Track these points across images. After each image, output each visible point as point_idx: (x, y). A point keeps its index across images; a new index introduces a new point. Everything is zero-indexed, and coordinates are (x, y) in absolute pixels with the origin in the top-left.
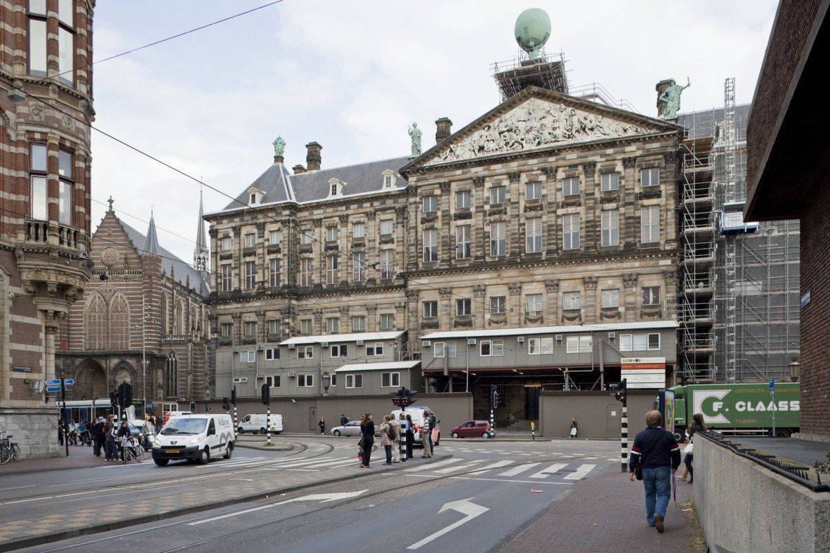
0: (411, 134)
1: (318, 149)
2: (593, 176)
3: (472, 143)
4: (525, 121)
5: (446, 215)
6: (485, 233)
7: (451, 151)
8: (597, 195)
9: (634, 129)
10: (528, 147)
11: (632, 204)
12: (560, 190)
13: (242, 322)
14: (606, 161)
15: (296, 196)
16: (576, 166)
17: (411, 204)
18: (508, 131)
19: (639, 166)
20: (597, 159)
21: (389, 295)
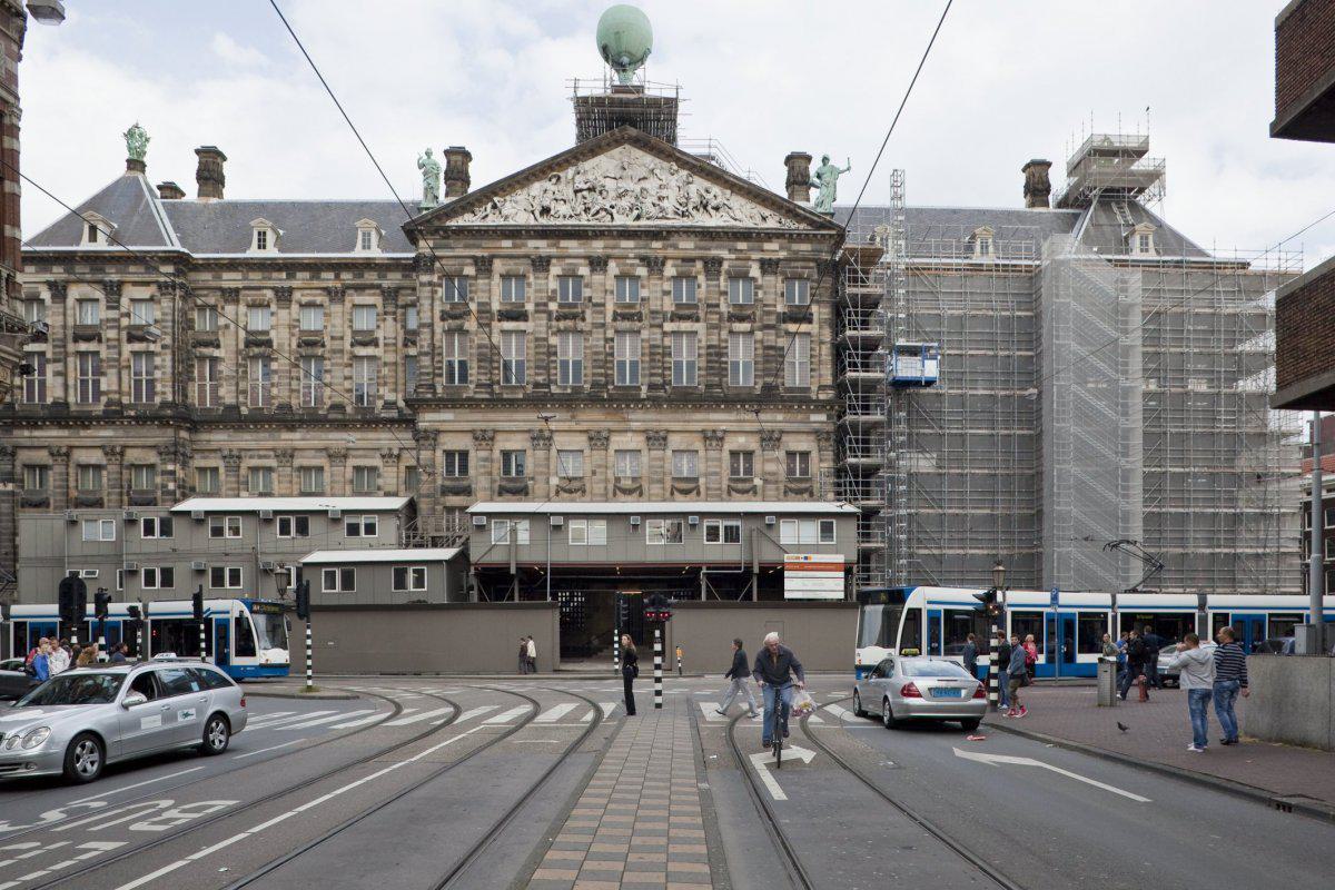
0: (421, 166)
1: (219, 160)
2: (718, 279)
3: (531, 199)
5: (484, 309)
6: (549, 346)
7: (495, 207)
8: (723, 308)
10: (621, 220)
12: (667, 293)
13: (71, 465)
14: (737, 259)
15: (180, 239)
16: (692, 260)
17: (422, 284)
18: (589, 189)
19: (783, 273)
20: (724, 254)
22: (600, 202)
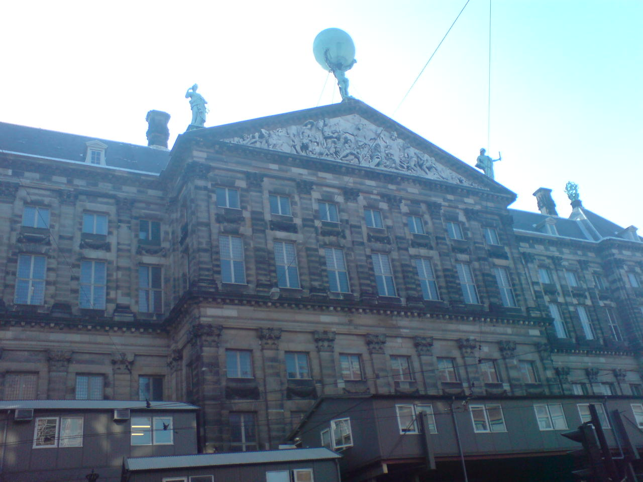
5: (257, 218)
6: (320, 257)
11: (484, 259)
20: (439, 201)
21: (101, 339)
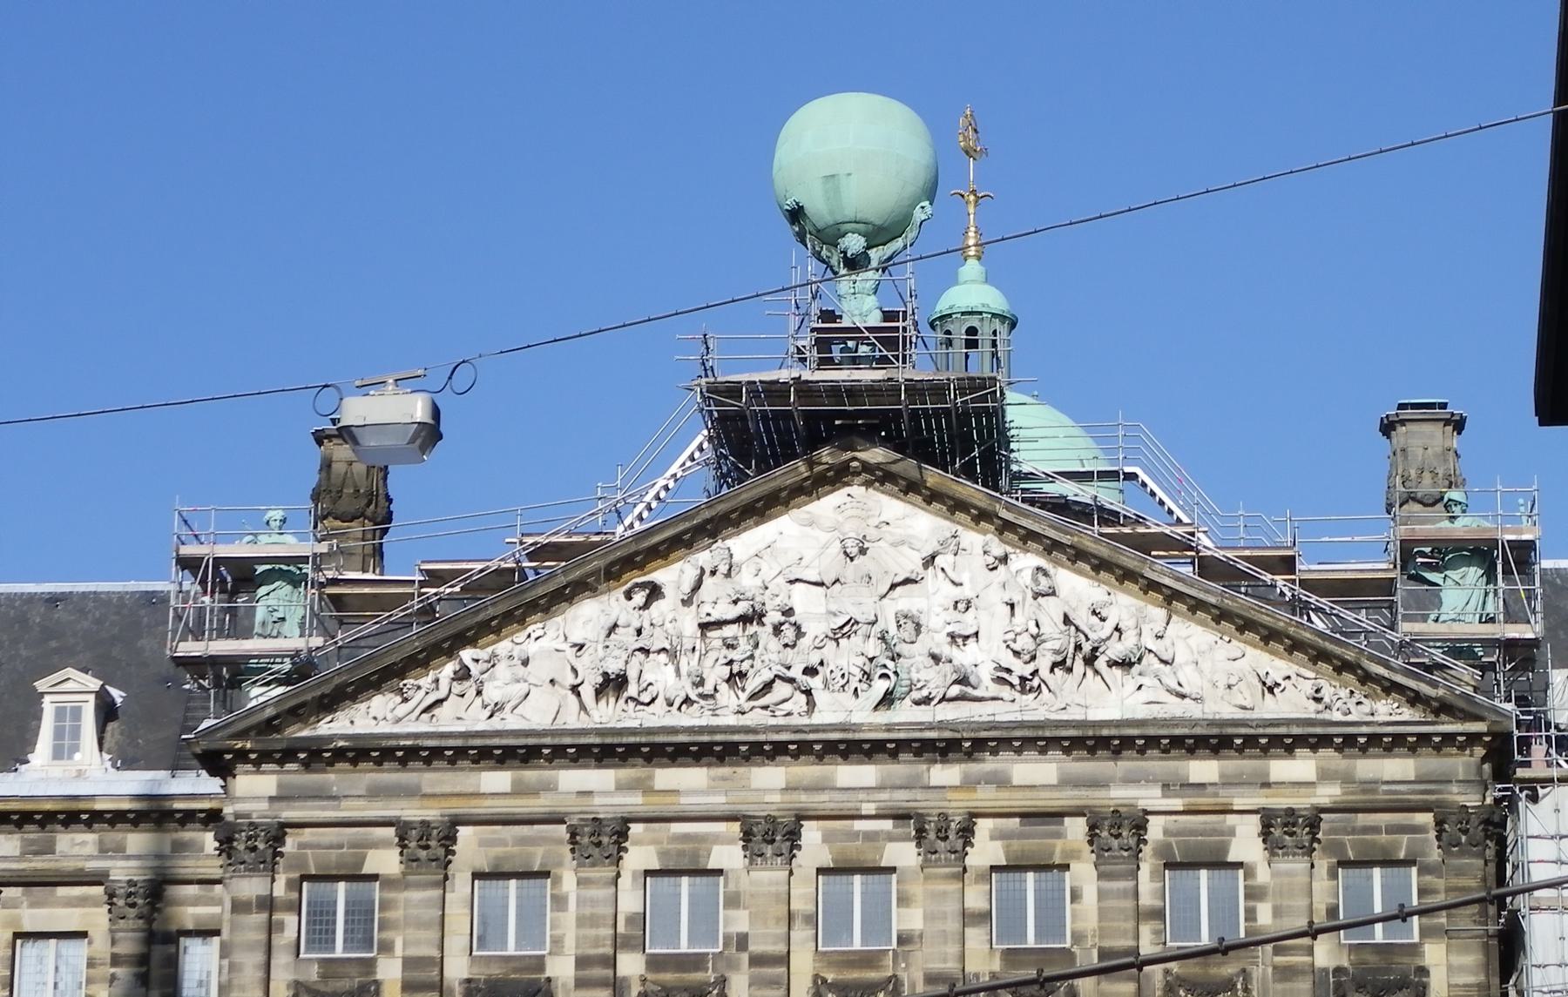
2: (1134, 874)
4: (822, 584)
7: (463, 674)
9: (1308, 687)
10: (838, 709)
12: (969, 918)
16: (1057, 815)
20: (1149, 797)
22: (770, 656)
